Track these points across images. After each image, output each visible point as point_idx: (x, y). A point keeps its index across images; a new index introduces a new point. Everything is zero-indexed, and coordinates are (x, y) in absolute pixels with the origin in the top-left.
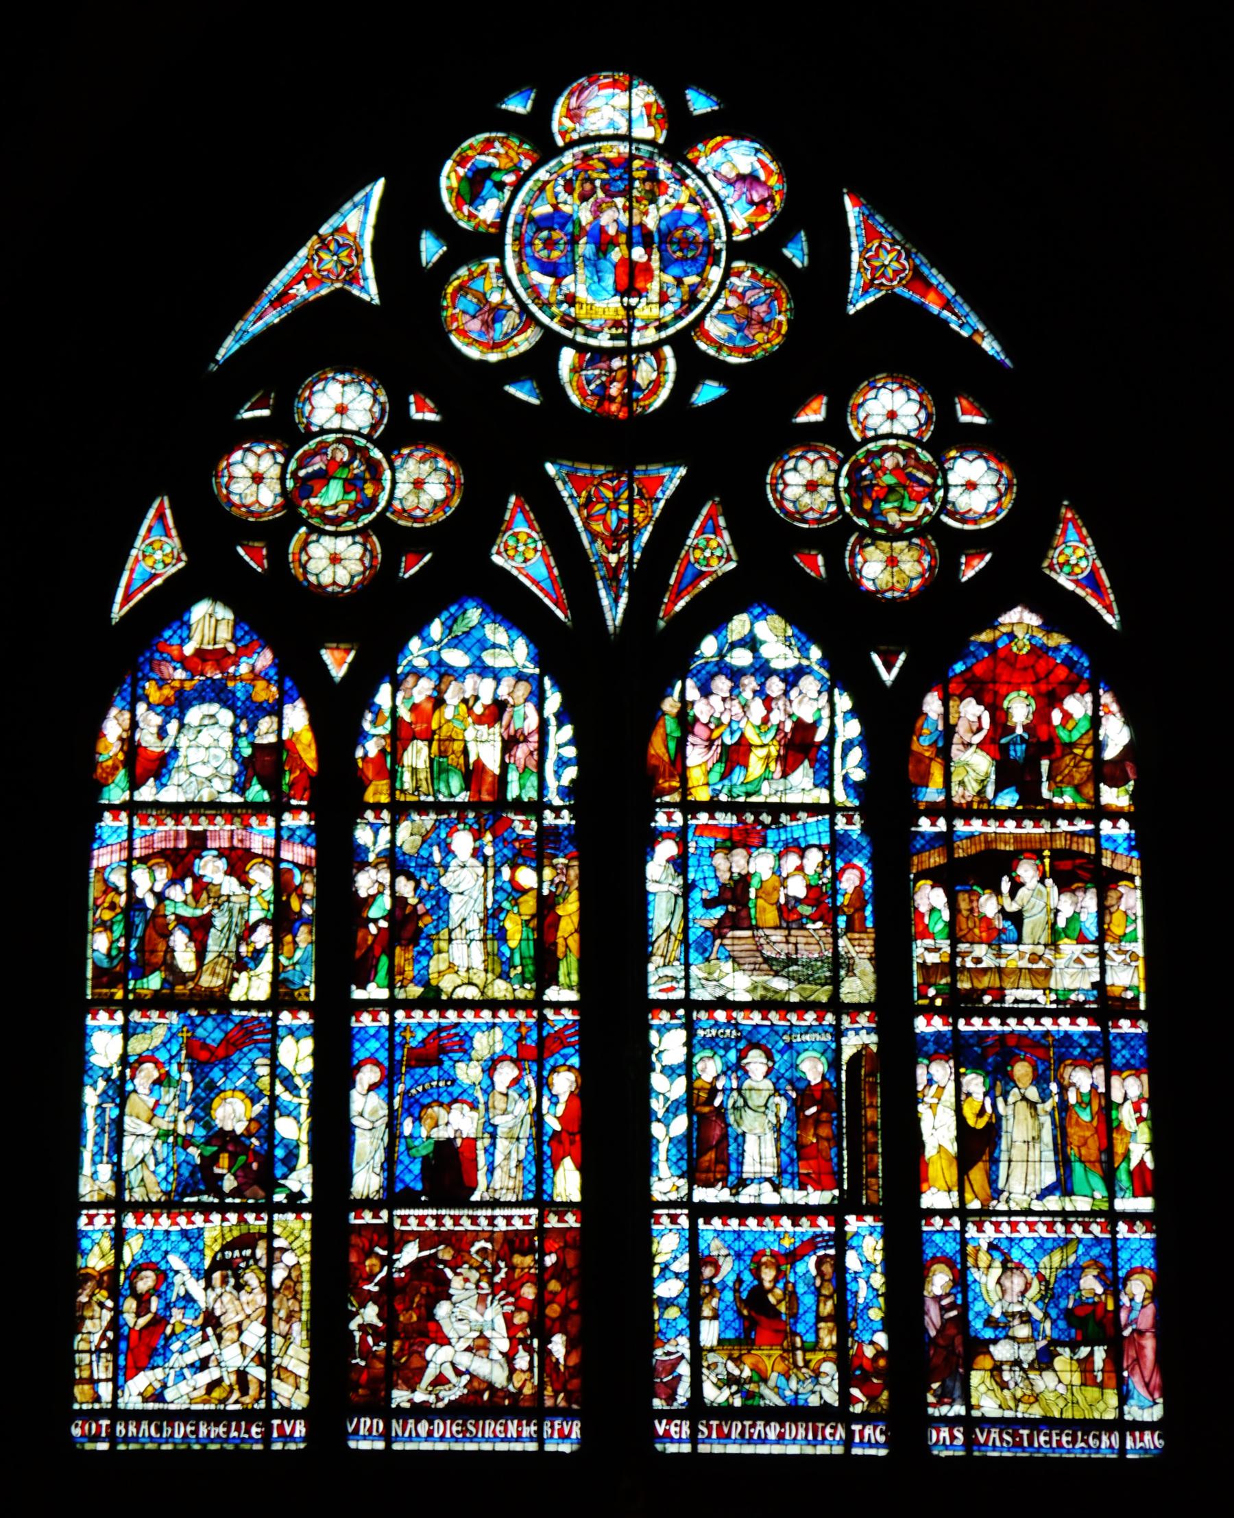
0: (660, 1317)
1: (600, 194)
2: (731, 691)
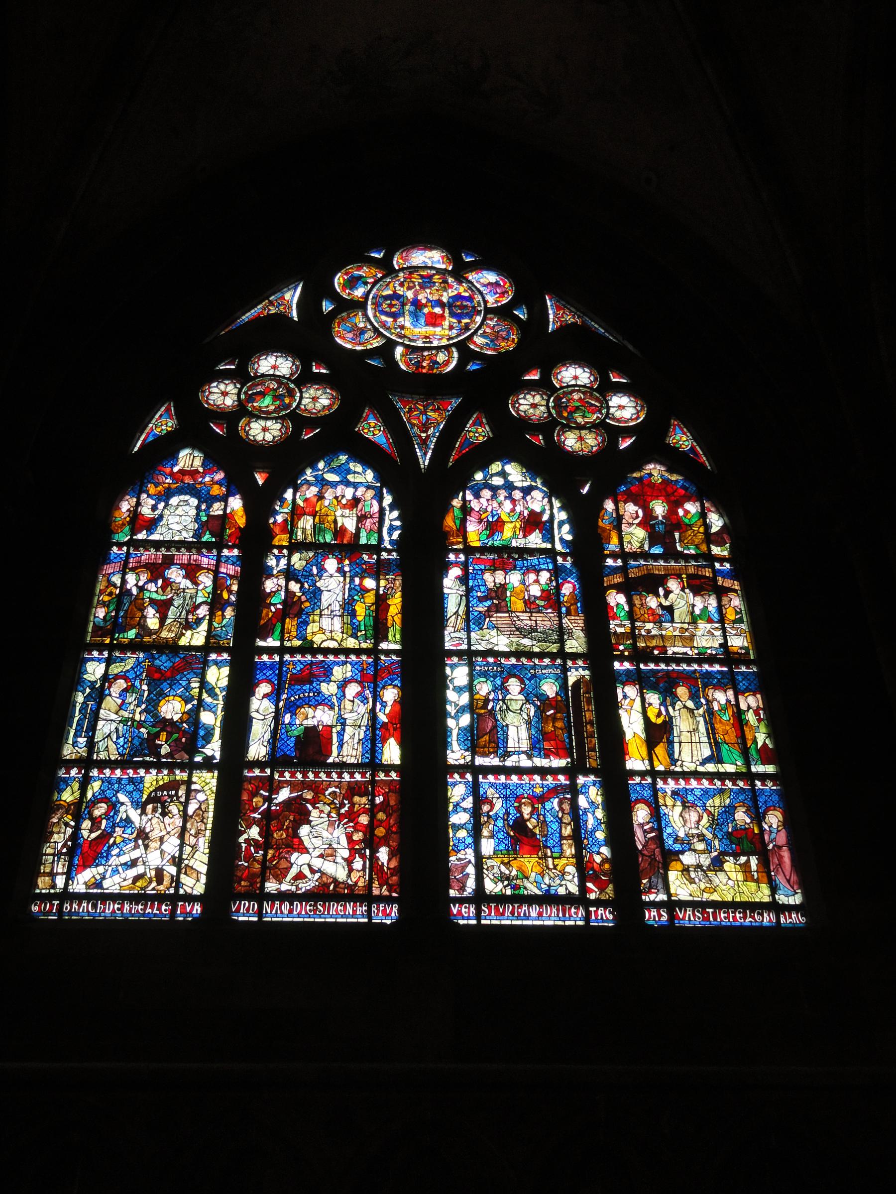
0: (454, 836)
1: (418, 287)
2: (492, 496)
